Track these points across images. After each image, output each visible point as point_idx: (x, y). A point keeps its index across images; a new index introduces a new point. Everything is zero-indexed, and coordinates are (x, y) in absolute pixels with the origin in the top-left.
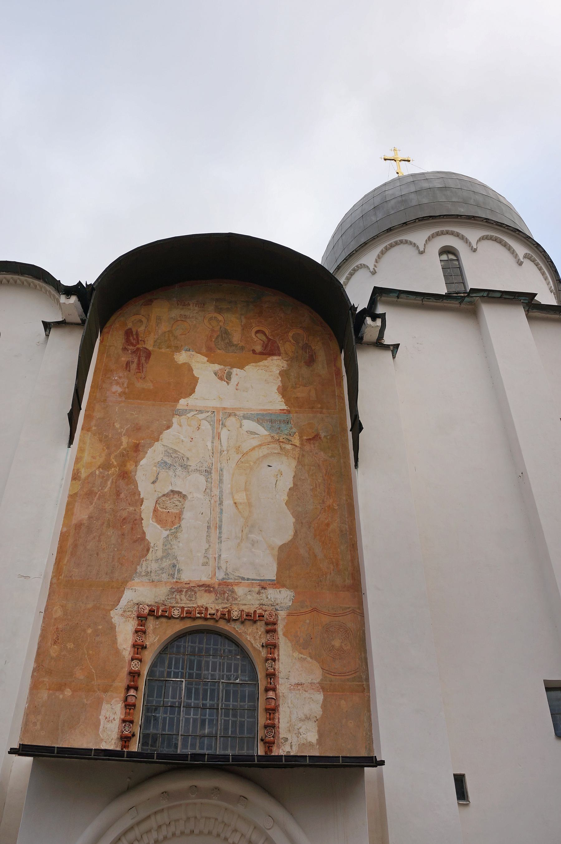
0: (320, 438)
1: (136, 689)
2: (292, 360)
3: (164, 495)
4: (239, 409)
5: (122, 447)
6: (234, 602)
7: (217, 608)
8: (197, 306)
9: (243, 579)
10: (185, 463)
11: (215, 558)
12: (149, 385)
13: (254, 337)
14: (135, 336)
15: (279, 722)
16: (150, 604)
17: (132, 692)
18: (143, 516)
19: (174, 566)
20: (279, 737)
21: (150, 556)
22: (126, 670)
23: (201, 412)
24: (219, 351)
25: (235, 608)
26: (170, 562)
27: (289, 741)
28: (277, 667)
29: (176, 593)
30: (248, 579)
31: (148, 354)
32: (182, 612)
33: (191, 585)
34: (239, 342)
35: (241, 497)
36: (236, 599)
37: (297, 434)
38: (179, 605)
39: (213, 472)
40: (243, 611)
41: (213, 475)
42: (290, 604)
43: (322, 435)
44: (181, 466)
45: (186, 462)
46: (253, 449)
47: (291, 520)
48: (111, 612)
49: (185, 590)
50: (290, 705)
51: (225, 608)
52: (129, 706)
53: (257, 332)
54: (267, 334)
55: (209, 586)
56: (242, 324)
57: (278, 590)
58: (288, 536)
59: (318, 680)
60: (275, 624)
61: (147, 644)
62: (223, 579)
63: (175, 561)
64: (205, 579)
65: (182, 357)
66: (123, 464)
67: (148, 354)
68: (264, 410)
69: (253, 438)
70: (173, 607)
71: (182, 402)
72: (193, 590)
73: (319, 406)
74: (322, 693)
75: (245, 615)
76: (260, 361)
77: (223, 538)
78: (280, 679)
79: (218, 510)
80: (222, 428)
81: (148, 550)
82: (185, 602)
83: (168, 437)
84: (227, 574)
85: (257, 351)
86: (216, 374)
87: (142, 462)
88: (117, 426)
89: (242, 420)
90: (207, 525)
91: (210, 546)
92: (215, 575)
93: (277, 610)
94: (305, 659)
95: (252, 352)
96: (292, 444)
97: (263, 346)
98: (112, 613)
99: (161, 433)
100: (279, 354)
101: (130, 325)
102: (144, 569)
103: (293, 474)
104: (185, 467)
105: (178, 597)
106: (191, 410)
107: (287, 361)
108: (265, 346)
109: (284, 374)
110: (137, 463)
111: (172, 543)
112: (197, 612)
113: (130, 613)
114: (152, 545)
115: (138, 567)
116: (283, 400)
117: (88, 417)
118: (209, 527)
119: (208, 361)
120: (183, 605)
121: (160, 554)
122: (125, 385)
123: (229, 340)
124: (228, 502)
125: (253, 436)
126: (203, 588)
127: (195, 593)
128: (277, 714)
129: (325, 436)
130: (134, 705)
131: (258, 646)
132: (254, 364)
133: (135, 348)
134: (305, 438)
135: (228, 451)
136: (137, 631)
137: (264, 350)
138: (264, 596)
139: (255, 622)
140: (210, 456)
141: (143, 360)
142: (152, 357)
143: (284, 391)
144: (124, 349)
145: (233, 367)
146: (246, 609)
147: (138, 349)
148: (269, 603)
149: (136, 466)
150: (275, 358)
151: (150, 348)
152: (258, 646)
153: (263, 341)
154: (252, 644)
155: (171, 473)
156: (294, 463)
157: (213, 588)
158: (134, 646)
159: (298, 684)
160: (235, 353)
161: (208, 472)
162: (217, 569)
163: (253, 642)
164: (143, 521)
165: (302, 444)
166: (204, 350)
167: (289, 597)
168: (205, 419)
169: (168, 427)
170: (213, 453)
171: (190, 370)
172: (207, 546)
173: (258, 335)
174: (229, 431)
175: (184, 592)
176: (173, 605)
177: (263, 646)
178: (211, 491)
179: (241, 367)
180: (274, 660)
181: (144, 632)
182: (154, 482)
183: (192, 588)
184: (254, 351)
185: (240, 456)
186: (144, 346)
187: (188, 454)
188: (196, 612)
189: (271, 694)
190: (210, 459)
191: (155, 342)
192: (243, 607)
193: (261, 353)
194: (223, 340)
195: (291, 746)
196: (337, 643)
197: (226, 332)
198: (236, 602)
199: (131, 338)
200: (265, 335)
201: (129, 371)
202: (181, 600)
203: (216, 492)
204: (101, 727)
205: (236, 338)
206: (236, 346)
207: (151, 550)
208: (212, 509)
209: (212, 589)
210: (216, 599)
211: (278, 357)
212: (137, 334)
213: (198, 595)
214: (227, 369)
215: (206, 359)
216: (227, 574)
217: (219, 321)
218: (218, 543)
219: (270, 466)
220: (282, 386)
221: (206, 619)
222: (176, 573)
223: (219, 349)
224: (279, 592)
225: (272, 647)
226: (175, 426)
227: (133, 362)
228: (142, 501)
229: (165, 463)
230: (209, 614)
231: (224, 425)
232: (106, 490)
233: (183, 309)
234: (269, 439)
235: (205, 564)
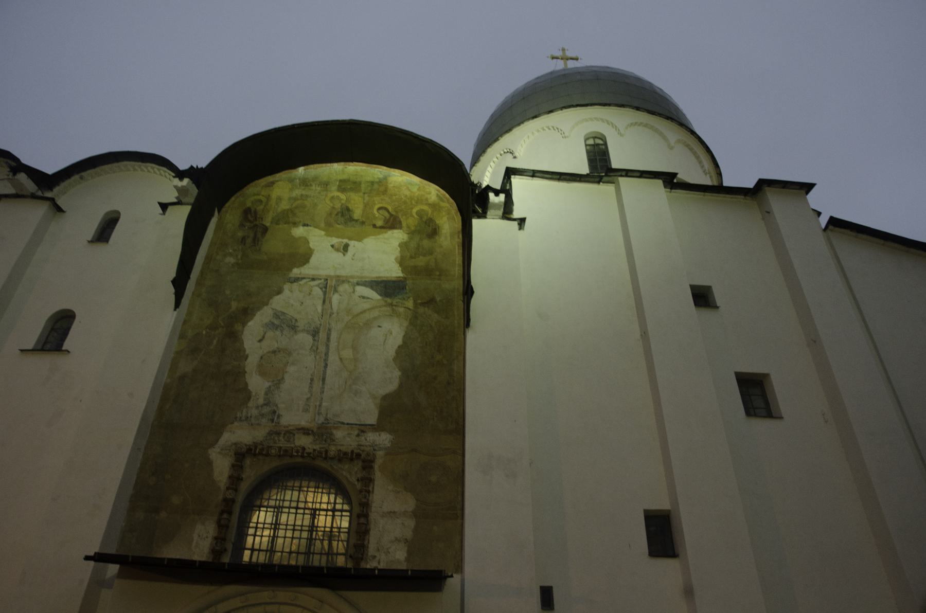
0: (436, 302)
3: (269, 352)
4: (352, 277)
5: (231, 310)
6: (332, 443)
7: (315, 448)
8: (320, 186)
9: (343, 423)
10: (293, 324)
11: (316, 406)
12: (265, 257)
13: (375, 211)
14: (253, 215)
15: (369, 543)
16: (248, 443)
17: (225, 516)
18: (246, 369)
19: (274, 412)
20: (367, 555)
21: (250, 404)
22: (221, 497)
23: (313, 279)
24: (338, 226)
25: (333, 448)
26: (270, 409)
27: (377, 559)
28: (370, 498)
29: (274, 435)
30: (348, 424)
31: (265, 230)
32: (280, 451)
33: (290, 428)
34: (360, 218)
35: (347, 354)
36: (334, 441)
37: (411, 298)
38: (276, 445)
39: (321, 331)
40: (340, 450)
41: (320, 334)
42: (389, 445)
43: (438, 299)
44: (289, 327)
45: (295, 323)
46: (365, 311)
47: (397, 373)
48: (209, 450)
49: (283, 432)
50: (381, 529)
51: (322, 448)
54: (390, 210)
55: (308, 429)
56: (365, 201)
57: (377, 434)
58: (393, 387)
59: (411, 509)
60: (372, 461)
61: (244, 476)
62: (323, 423)
63: (275, 408)
64: (303, 424)
67: (265, 230)
68: (379, 277)
69: (365, 302)
70: (271, 447)
71: (296, 272)
72: (291, 433)
73: (438, 273)
74: (414, 519)
75: (342, 454)
76: (379, 234)
77: (325, 390)
78: (373, 508)
79: (323, 364)
80: (333, 294)
81: (249, 398)
82: (282, 442)
83: (278, 302)
84: (326, 419)
85: (377, 225)
86: (332, 246)
87: (250, 324)
88: (228, 292)
89: (355, 286)
90: (310, 377)
91: (311, 395)
92: (315, 420)
93: (374, 450)
94: (399, 492)
95: (372, 226)
96: (405, 307)
97: (384, 221)
98: (210, 451)
99: (271, 297)
100: (401, 228)
101: (249, 204)
102: (244, 414)
103: (402, 334)
105: (276, 438)
106: (304, 278)
107: (406, 233)
108: (387, 221)
109: (403, 246)
110: (244, 324)
111: (273, 392)
112: (294, 451)
113: (228, 451)
114: (254, 394)
115: (238, 413)
116: (400, 269)
117: (199, 283)
118: (312, 380)
119: (325, 235)
120: (282, 445)
121: (261, 401)
122: (239, 257)
123: (350, 216)
124: (333, 357)
125: (365, 300)
126: (301, 431)
127: (294, 435)
128: (367, 537)
129: (440, 301)
130: (227, 527)
131: (353, 479)
132: (373, 237)
133: (252, 225)
134: (419, 301)
135: (338, 313)
136: (233, 466)
137: (386, 224)
138: (363, 438)
139: (352, 460)
140: (319, 318)
142: (269, 232)
143: (401, 262)
144: (242, 225)
145: (350, 239)
146: (344, 449)
147: (256, 226)
148: (367, 444)
149: (244, 327)
150: (395, 231)
151: (268, 224)
152: (353, 479)
153: (385, 217)
154: (347, 479)
155: (278, 333)
156: (406, 324)
157: (312, 431)
158: (230, 477)
159: (391, 512)
160: (354, 227)
161: (315, 333)
162: (317, 415)
163: (348, 476)
164: (246, 374)
166: (323, 225)
167: (388, 440)
168: (316, 286)
169: (279, 292)
170: (322, 316)
171: (307, 242)
172: (309, 395)
173: (381, 211)
174: (341, 295)
175: (282, 435)
176: (271, 445)
177: (358, 480)
178: (317, 348)
179: (359, 239)
180: (369, 492)
181: (242, 467)
182: (260, 341)
183: (291, 431)
184: (374, 226)
185: (350, 318)
186: (261, 222)
187: (296, 316)
188: (292, 451)
189: (362, 520)
190: (319, 320)
191: (273, 218)
192: (339, 448)
193: (381, 227)
194: (343, 215)
195: (379, 563)
196: (433, 479)
197: (348, 209)
198: (334, 443)
199: (249, 216)
200: (388, 211)
201: (244, 244)
202: (279, 441)
203: (322, 349)
204: (195, 542)
206: (357, 221)
207: (252, 399)
208: (316, 364)
209: (310, 432)
210: (314, 441)
211: (399, 231)
212: (256, 212)
213: (297, 436)
214: (345, 241)
215: (323, 233)
216: (326, 419)
217: (340, 199)
218: (321, 393)
219: (379, 326)
220: (401, 256)
221: (302, 456)
222: (276, 418)
223: (339, 224)
224: (378, 435)
225: (368, 481)
226: (286, 292)
227: (248, 237)
228: (247, 356)
229: (273, 323)
230: (307, 453)
231: (336, 291)
232: (212, 347)
233: (304, 189)
234: (383, 303)
235: (306, 410)
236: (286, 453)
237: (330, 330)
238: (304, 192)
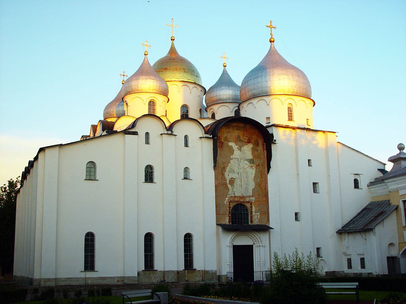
1: (230, 214)
2: (254, 144)
23: (236, 159)
52: (229, 217)
53: (246, 136)
60: (252, 203)
65: (230, 144)
66: (222, 172)
71: (232, 157)
104: (234, 172)
109: (253, 149)
141: (222, 144)
143: (252, 154)
150: (250, 144)
151: (223, 141)
165: (256, 167)
182: (228, 176)
193: (247, 143)
205: (242, 138)
225: (251, 207)
236: (237, 201)
237: (241, 173)
238: (229, 130)
